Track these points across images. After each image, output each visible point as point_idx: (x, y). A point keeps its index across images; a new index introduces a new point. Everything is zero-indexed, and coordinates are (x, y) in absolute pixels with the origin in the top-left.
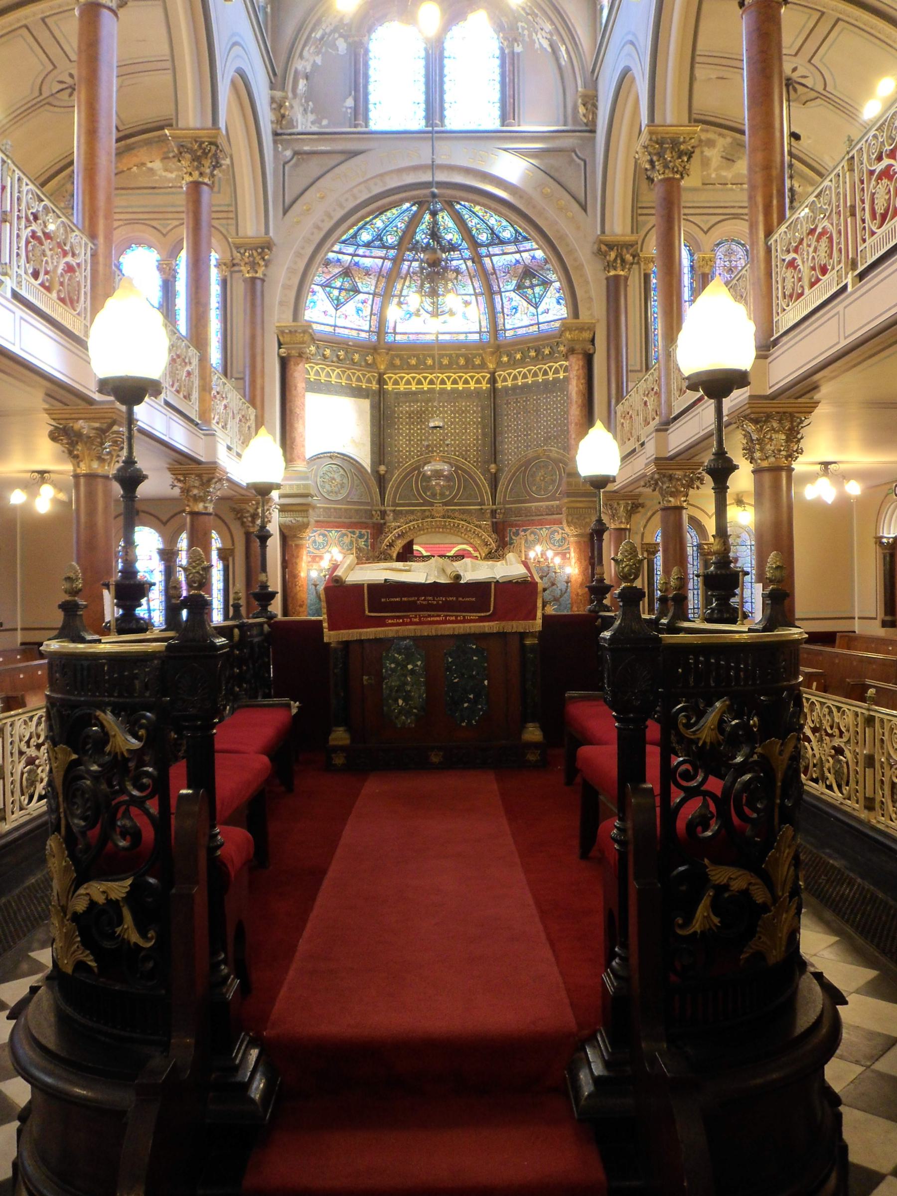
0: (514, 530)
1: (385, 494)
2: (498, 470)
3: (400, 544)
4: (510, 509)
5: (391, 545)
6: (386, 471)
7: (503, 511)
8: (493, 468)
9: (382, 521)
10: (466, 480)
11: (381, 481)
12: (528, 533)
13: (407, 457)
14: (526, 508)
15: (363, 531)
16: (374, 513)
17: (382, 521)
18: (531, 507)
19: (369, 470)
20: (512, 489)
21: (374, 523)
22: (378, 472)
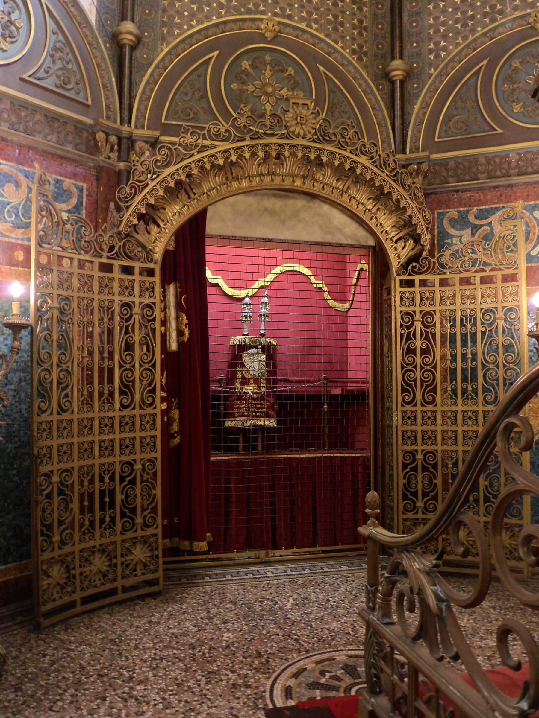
0: (453, 213)
1: (132, 99)
2: (408, 75)
3: (176, 214)
4: (444, 163)
5: (149, 217)
6: (139, 40)
7: (425, 166)
8: (397, 68)
9: (122, 165)
10: (334, 90)
11: (123, 58)
12: (494, 219)
13: (192, 15)
14: (489, 159)
15: (68, 183)
16: (100, 136)
17: (122, 165)
18: (505, 156)
19: (92, 17)
20: (448, 118)
21: (100, 169)
22: (115, 39)
